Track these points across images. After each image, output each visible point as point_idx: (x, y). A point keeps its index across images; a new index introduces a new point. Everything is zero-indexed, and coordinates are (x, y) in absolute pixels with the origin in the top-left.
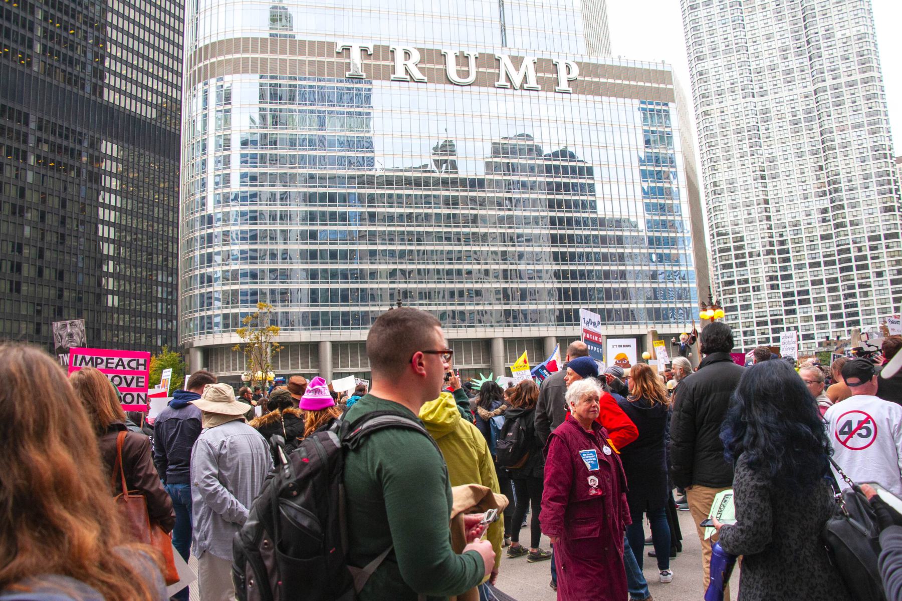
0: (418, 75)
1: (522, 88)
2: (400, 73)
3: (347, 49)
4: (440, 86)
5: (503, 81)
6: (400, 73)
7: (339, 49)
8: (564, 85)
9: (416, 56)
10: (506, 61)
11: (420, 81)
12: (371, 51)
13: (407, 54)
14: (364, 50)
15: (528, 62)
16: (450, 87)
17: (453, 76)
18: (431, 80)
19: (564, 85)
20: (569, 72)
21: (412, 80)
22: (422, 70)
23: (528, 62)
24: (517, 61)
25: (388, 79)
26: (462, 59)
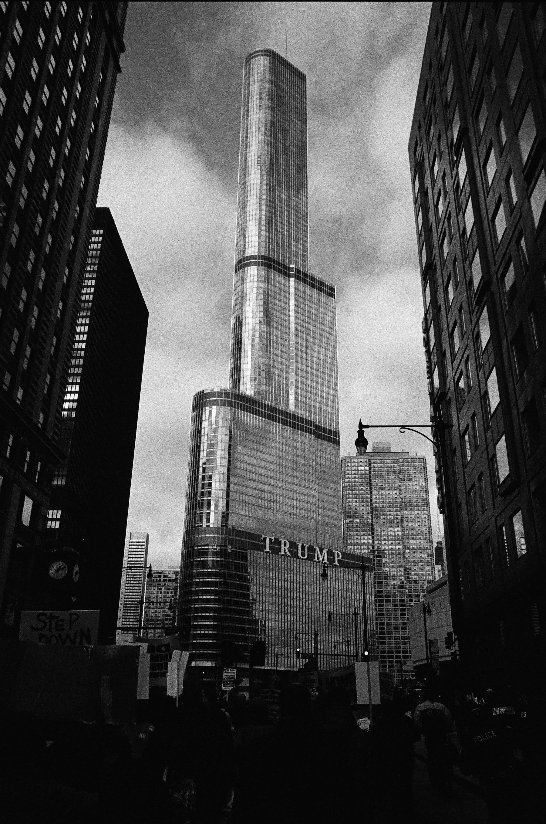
0: (289, 554)
1: (322, 562)
2: (282, 552)
3: (265, 539)
4: (295, 559)
5: (316, 559)
6: (282, 553)
7: (262, 538)
8: (336, 563)
9: (288, 545)
10: (318, 549)
11: (289, 556)
12: (273, 541)
13: (285, 545)
14: (271, 540)
15: (325, 551)
16: (298, 560)
17: (300, 556)
18: (292, 557)
19: (336, 563)
20: (338, 557)
21: (286, 555)
22: (289, 550)
23: (325, 551)
24: (321, 550)
25: (278, 554)
26: (303, 548)
